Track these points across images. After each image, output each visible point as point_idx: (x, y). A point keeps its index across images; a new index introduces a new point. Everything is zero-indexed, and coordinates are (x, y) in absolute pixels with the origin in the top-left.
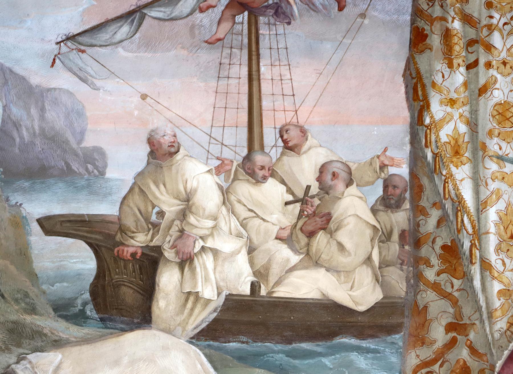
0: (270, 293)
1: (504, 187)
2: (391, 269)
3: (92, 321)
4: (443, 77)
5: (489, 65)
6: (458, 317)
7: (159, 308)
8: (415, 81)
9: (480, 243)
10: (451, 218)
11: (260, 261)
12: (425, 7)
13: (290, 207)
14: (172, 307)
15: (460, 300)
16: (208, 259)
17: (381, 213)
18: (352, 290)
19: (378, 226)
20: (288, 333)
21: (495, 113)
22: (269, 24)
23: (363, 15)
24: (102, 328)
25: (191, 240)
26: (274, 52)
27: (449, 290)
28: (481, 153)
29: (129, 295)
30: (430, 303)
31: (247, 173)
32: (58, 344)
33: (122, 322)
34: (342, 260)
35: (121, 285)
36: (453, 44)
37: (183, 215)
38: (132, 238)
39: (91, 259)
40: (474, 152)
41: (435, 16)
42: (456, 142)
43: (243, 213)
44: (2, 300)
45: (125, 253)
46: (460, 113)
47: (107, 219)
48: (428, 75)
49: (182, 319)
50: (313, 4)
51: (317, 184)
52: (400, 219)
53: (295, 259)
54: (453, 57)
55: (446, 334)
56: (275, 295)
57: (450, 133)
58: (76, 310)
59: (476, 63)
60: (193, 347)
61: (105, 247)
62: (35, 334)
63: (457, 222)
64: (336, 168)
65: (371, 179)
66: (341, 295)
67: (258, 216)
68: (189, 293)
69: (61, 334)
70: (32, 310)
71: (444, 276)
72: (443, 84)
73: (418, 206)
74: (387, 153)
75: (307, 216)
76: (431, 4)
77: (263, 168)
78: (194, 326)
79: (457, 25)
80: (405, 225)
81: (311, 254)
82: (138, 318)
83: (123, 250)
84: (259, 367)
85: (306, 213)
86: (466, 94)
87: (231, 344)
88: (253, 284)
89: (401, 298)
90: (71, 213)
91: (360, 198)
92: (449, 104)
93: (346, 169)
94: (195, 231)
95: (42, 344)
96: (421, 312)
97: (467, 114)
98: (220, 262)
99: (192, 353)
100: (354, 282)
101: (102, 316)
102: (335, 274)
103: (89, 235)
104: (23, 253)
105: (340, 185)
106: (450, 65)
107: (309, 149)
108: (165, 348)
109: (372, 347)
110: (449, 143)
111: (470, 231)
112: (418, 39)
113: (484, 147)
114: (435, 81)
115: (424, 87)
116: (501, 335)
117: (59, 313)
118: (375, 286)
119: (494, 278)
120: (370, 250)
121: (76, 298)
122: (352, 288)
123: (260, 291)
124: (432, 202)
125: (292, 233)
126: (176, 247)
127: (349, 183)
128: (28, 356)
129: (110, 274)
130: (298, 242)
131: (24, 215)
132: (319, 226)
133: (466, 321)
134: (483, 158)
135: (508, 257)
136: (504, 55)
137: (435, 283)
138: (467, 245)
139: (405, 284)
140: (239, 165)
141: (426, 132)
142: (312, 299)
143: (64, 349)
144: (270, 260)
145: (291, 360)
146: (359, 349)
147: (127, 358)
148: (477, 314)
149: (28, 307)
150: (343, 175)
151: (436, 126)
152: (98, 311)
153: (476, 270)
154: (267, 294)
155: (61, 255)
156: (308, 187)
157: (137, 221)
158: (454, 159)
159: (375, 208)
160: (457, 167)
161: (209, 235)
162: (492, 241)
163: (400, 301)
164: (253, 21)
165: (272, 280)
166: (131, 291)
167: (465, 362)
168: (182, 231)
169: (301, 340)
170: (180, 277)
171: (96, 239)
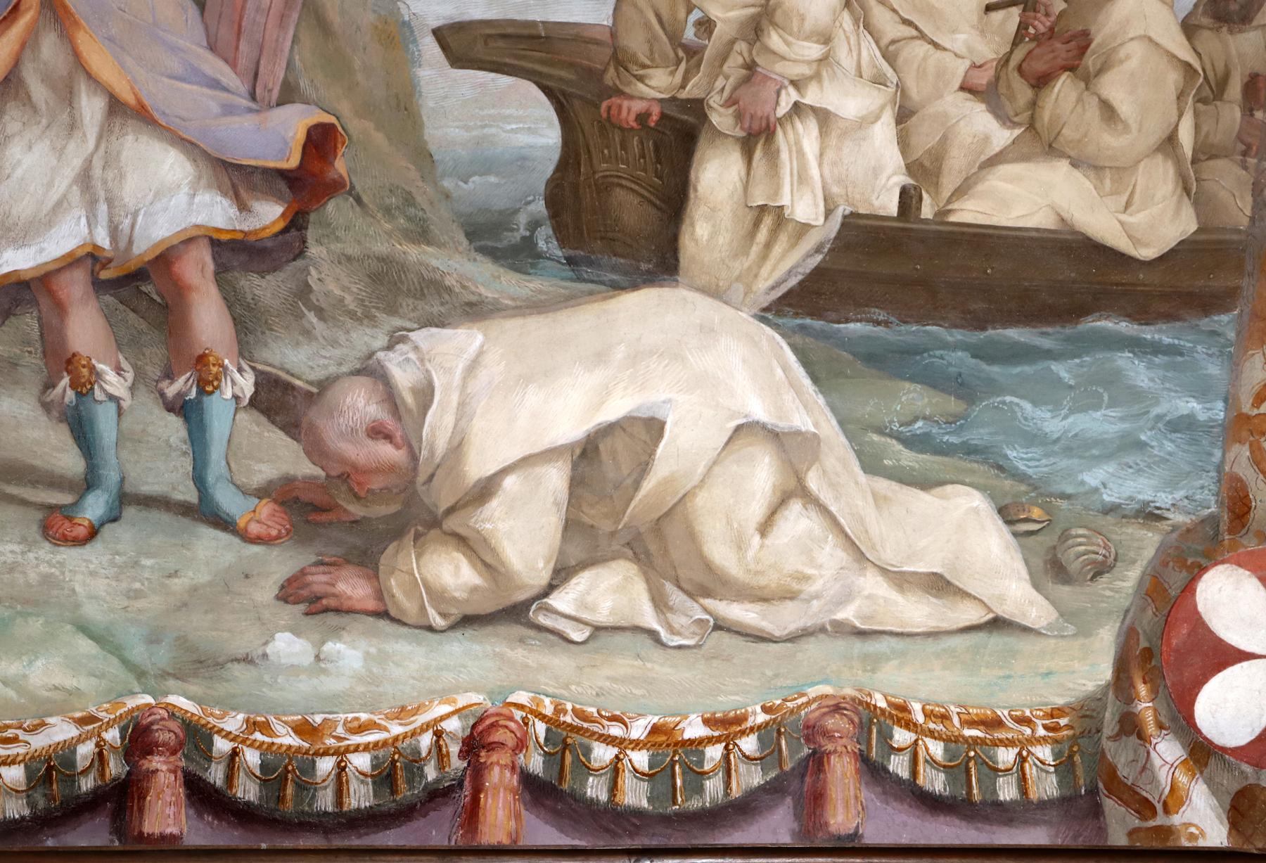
0: (943, 213)
2: (1220, 164)
3: (549, 263)
7: (696, 241)
11: (924, 140)
13: (997, 16)
14: (724, 239)
16: (807, 135)
17: (1206, 34)
18: (1129, 211)
19: (1196, 64)
20: (978, 306)
24: (572, 280)
25: (773, 87)
29: (630, 208)
32: (476, 311)
33: (614, 269)
34: (1111, 142)
35: (613, 184)
37: (755, 29)
38: (641, 79)
39: (550, 124)
43: (890, 28)
44: (358, 209)
45: (624, 113)
47: (586, 34)
49: (746, 265)
53: (1002, 137)
56: (953, 218)
58: (516, 237)
60: (768, 330)
61: (581, 98)
62: (428, 287)
66: (1102, 221)
67: (922, 36)
68: (763, 209)
69: (482, 290)
70: (422, 234)
75: (1035, 38)
78: (770, 282)
81: (1038, 125)
82: (649, 261)
83: (620, 107)
84: (912, 379)
85: (1031, 30)
87: (851, 326)
88: (904, 192)
89: (1239, 232)
90: (508, 17)
94: (780, 67)
95: (442, 309)
98: (833, 140)
99: (764, 343)
100: (1132, 193)
101: (571, 252)
102: (1092, 174)
103: (545, 70)
104: (402, 105)
108: (707, 330)
109: (1167, 340)
117: (478, 244)
118: (1179, 202)
120: (1175, 118)
121: (516, 211)
123: (919, 209)
125: (997, 78)
126: (735, 102)
128: (411, 334)
129: (590, 158)
130: (1012, 98)
131: (407, 18)
132: (1060, 62)
139: (1249, 199)
142: (1037, 230)
143: (487, 322)
144: (944, 139)
145: (984, 366)
147: (622, 347)
149: (412, 227)
152: (563, 243)
154: (936, 215)
155: (485, 112)
157: (652, 41)
159: (1193, 21)
161: (811, 78)
163: (1235, 237)
165: (949, 183)
166: (636, 200)
168: (751, 67)
170: (743, 173)
171: (561, 79)
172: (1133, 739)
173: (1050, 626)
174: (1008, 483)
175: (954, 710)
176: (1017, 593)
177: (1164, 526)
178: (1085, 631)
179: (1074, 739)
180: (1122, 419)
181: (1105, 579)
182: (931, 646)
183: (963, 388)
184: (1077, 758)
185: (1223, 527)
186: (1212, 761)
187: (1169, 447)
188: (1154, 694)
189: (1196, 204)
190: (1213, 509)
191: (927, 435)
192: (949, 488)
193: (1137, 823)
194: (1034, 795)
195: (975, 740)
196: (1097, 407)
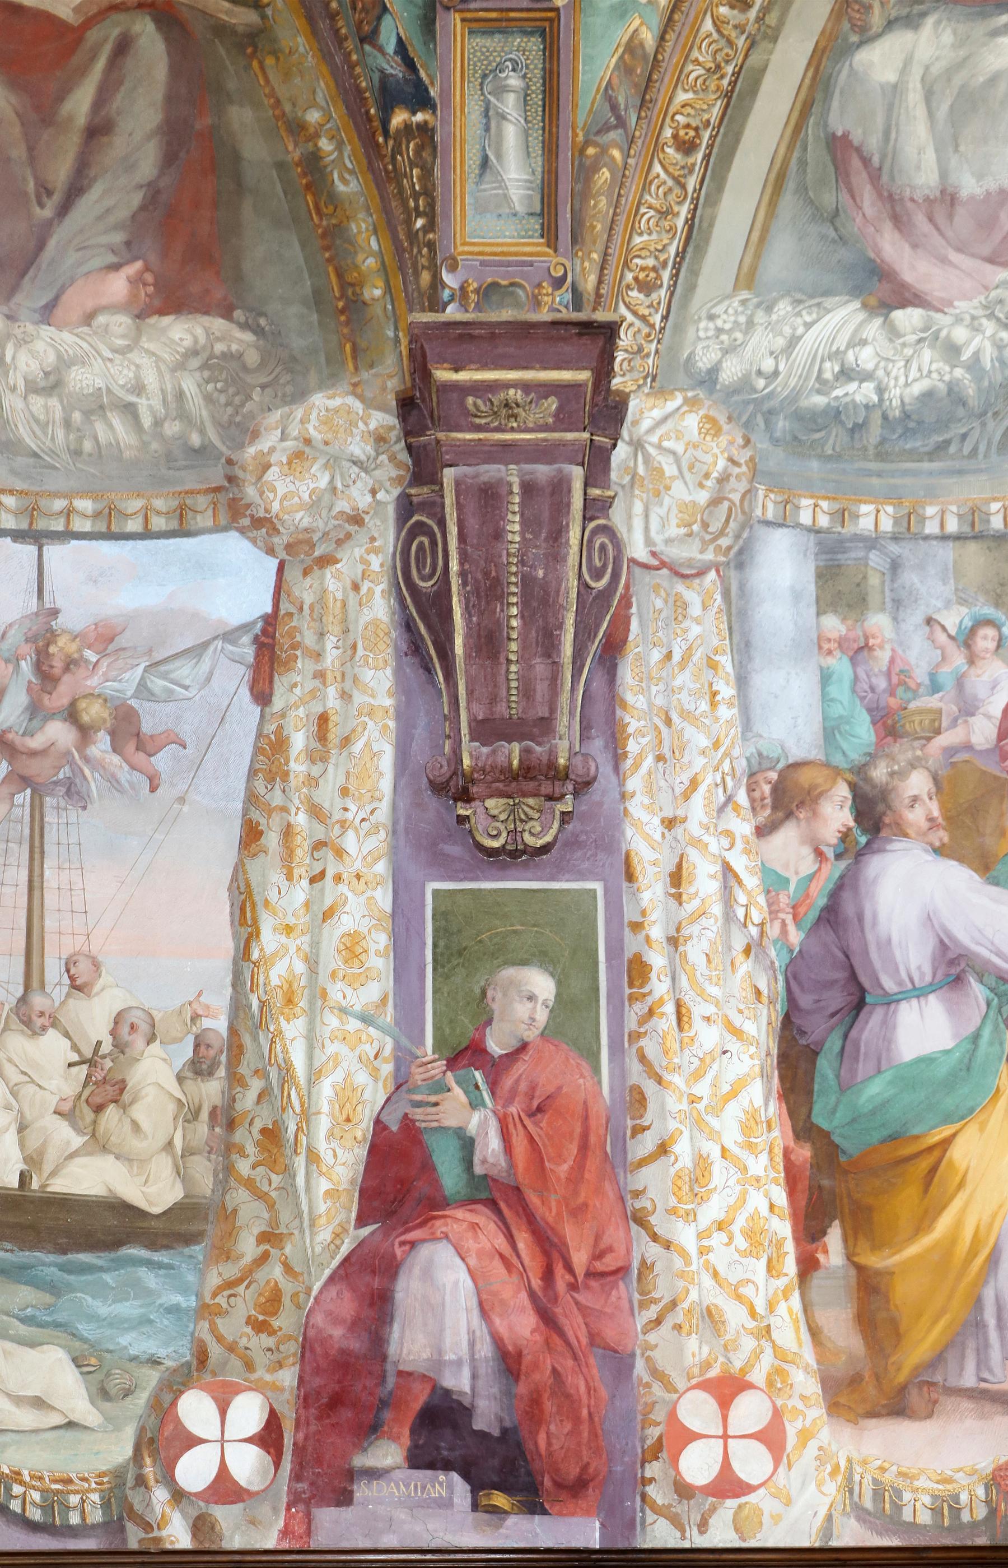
0: (44, 1186)
1: (344, 1050)
2: (196, 1158)
5: (338, 878)
8: (243, 897)
9: (308, 1126)
11: (34, 1143)
12: (262, 791)
13: (75, 1070)
17: (189, 1082)
19: (184, 1100)
20: (63, 1241)
21: (342, 947)
22: (58, 808)
23: (182, 800)
26: (63, 849)
27: (265, 1188)
28: (319, 1003)
31: (23, 1022)
34: (137, 1145)
40: (311, 1003)
43: (15, 1077)
50: (118, 782)
51: (110, 1038)
52: (211, 1090)
53: (77, 1141)
56: (49, 1189)
59: (323, 874)
64: (135, 1017)
65: (179, 1035)
66: (133, 1194)
67: (33, 1081)
71: (260, 1169)
73: (235, 1073)
74: (202, 999)
75: (96, 1083)
77: (42, 1014)
79: (301, 819)
80: (217, 1100)
84: (26, 1283)
86: (307, 918)
88: (22, 1174)
91: (164, 1060)
93: (149, 1021)
96: (229, 1216)
97: (306, 948)
105: (139, 1041)
106: (289, 877)
107: (103, 990)
109: (166, 1261)
111: (298, 1109)
112: (251, 835)
113: (324, 994)
116: (323, 1249)
119: (321, 1173)
122: (146, 1182)
125: (75, 1107)
127: (151, 1040)
130: (82, 1119)
132: (109, 1097)
133: (283, 1230)
135: (341, 1146)
136: (358, 864)
140: (11, 1009)
144: (44, 1144)
145: (65, 1276)
146: (149, 1263)
148: (297, 1222)
150: (144, 1027)
151: (267, 962)
153: (300, 1162)
156: (99, 1043)
158: (286, 1010)
159: (182, 1075)
162: (323, 1124)
163: (204, 1201)
164: (37, 802)
165: (48, 1168)
169: (78, 1251)
172: (142, 1489)
173: (99, 1426)
174: (78, 1344)
175: (46, 1474)
176: (80, 1405)
177: (162, 1368)
178: (118, 1429)
179: (111, 1489)
180: (141, 1306)
181: (129, 1399)
182: (34, 1437)
183: (54, 1289)
184: (113, 1500)
185: (193, 1368)
186: (184, 1500)
187: (166, 1322)
188: (154, 1462)
189: (183, 1181)
190: (188, 1358)
191: (33, 1316)
192: (45, 1347)
193: (143, 1535)
194: (89, 1521)
195: (58, 1491)
196: (127, 1300)
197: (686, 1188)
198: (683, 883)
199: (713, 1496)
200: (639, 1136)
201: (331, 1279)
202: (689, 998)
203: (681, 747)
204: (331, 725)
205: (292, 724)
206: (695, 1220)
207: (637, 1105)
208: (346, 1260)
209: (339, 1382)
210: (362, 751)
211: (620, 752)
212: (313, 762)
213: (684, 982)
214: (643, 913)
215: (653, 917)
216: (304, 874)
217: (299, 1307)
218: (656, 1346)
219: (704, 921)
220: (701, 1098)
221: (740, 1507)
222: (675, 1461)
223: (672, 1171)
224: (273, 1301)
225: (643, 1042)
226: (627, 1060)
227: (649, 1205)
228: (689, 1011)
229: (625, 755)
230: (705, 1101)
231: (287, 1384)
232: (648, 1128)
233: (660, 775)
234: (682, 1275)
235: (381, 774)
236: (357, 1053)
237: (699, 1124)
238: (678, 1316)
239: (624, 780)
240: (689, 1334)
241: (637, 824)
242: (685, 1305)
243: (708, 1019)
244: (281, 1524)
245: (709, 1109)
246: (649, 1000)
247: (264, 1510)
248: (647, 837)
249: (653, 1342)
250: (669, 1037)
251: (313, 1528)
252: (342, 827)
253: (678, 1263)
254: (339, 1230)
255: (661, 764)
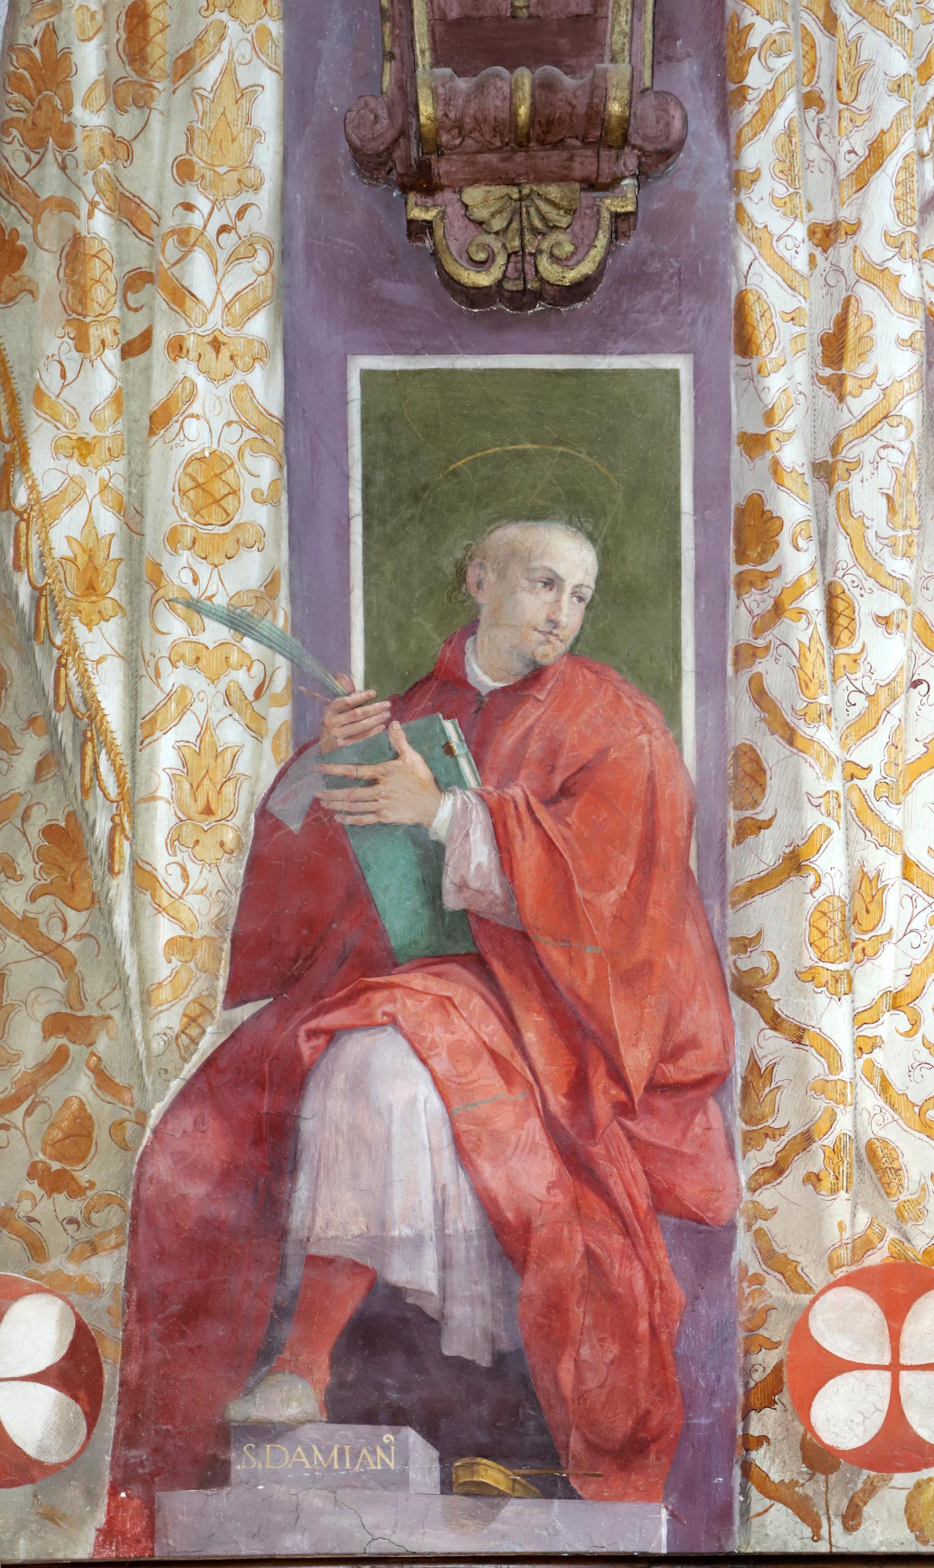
1: (197, 681)
4: (63, 376)
5: (177, 348)
6: (74, 1003)
10: (70, 757)
12: (20, 166)
15: (80, 960)
21: (189, 484)
28: (148, 591)
30: (13, 967)
36: (90, 282)
40: (133, 587)
41: (44, 196)
42: (91, 558)
46: (102, 480)
48: (26, 369)
54: (88, 320)
55: (46, 1038)
57: (76, 534)
59: (145, 340)
63: (83, 768)
71: (46, 902)
72: (62, 396)
76: (35, 158)
79: (100, 225)
86: (119, 427)
92: (76, 453)
97: (118, 483)
106: (81, 344)
110: (73, 561)
111: (113, 791)
113: (157, 576)
114: (42, 387)
115: (14, 401)
116: (168, 1044)
119: (160, 909)
124: (25, 716)
134: (154, 604)
135: (195, 858)
136: (215, 319)
137: (25, 918)
138: (103, 826)
141: (17, 529)
148: (117, 997)
153: (120, 889)
158: (84, 605)
160: (89, 625)
162: (162, 818)
167: (82, 1105)
197: (835, 933)
198: (849, 355)
199: (870, 1468)
200: (751, 840)
201: (183, 1097)
202: (850, 579)
203: (855, 75)
204: (153, 27)
205: (74, 24)
206: (850, 991)
207: (748, 783)
208: (210, 1063)
209: (201, 1276)
210: (217, 87)
211: (732, 87)
212: (120, 107)
213: (843, 551)
214: (769, 417)
215: (789, 424)
216: (110, 339)
217: (125, 1147)
218: (774, 1211)
219: (885, 432)
220: (869, 769)
221: (919, 1486)
222: (803, 1408)
223: (810, 902)
224: (78, 1136)
225: (761, 666)
226: (731, 699)
227: (765, 964)
228: (851, 605)
229: (742, 94)
230: (875, 776)
231: (106, 1280)
232: (767, 824)
233: (810, 137)
234: (822, 1088)
235: (257, 135)
236: (222, 687)
237: (863, 818)
238: (815, 1160)
239: (739, 147)
240: (834, 1191)
241: (762, 238)
242: (829, 1141)
243: (884, 621)
244: (101, 1518)
245: (883, 790)
246: (776, 585)
247: (71, 1496)
248: (781, 265)
249: (768, 1205)
250: (811, 657)
251: (158, 1524)
252: (182, 243)
253: (817, 1067)
254: (195, 1010)
255: (812, 113)
